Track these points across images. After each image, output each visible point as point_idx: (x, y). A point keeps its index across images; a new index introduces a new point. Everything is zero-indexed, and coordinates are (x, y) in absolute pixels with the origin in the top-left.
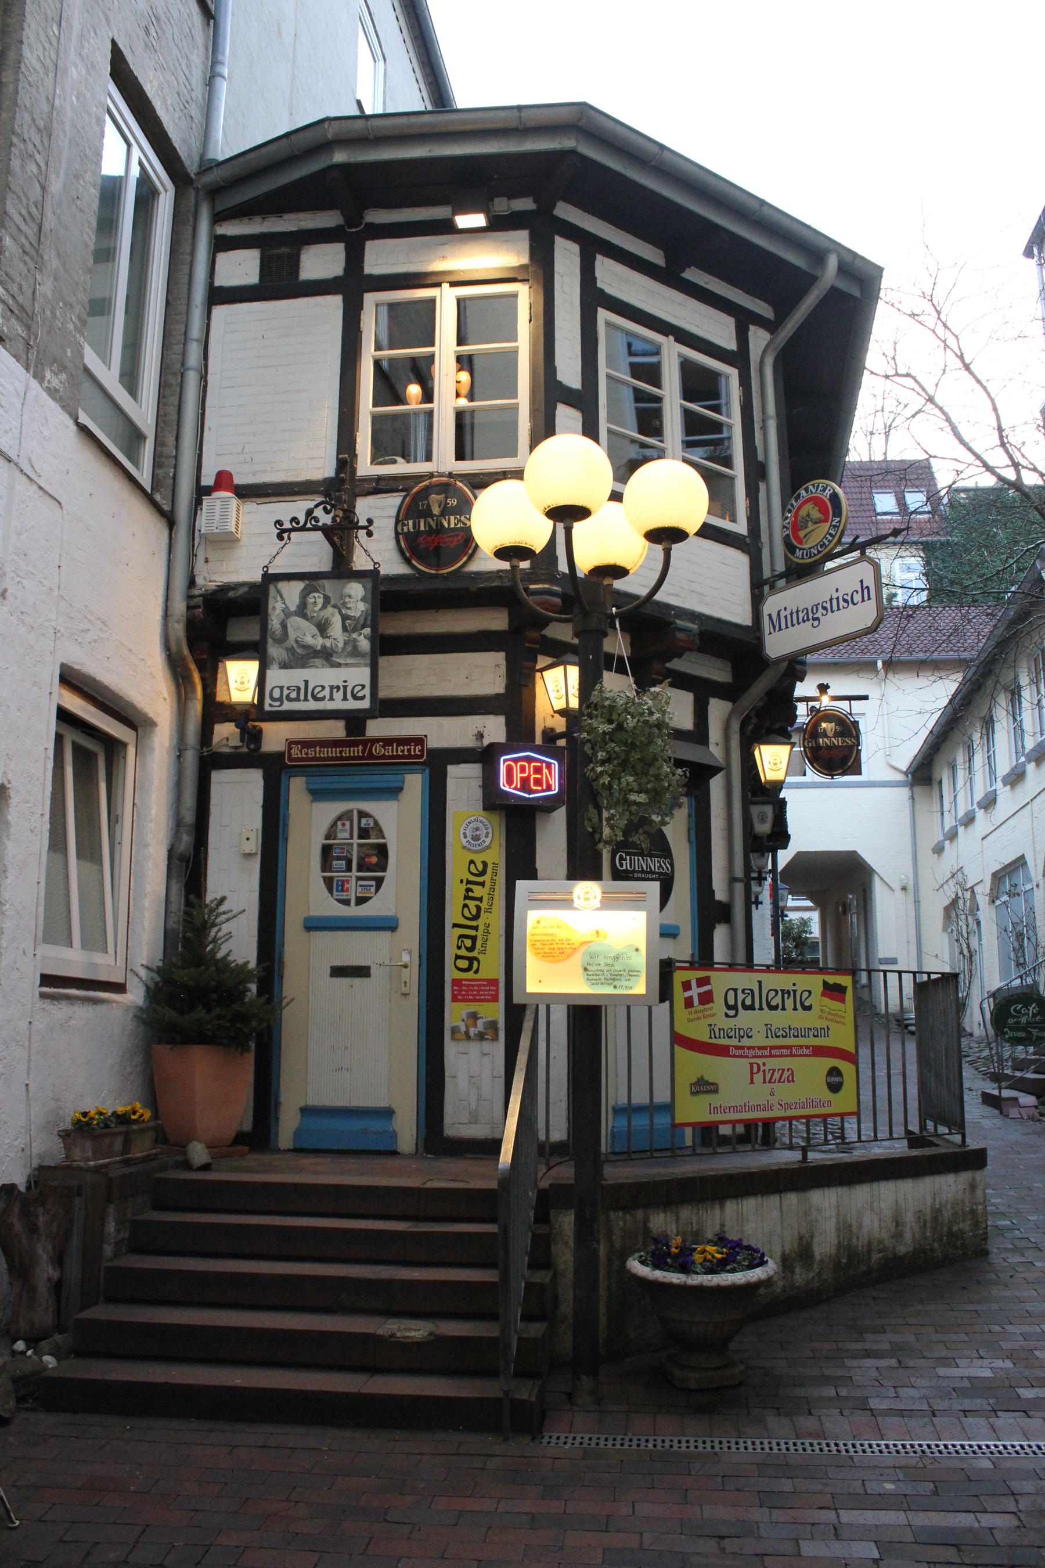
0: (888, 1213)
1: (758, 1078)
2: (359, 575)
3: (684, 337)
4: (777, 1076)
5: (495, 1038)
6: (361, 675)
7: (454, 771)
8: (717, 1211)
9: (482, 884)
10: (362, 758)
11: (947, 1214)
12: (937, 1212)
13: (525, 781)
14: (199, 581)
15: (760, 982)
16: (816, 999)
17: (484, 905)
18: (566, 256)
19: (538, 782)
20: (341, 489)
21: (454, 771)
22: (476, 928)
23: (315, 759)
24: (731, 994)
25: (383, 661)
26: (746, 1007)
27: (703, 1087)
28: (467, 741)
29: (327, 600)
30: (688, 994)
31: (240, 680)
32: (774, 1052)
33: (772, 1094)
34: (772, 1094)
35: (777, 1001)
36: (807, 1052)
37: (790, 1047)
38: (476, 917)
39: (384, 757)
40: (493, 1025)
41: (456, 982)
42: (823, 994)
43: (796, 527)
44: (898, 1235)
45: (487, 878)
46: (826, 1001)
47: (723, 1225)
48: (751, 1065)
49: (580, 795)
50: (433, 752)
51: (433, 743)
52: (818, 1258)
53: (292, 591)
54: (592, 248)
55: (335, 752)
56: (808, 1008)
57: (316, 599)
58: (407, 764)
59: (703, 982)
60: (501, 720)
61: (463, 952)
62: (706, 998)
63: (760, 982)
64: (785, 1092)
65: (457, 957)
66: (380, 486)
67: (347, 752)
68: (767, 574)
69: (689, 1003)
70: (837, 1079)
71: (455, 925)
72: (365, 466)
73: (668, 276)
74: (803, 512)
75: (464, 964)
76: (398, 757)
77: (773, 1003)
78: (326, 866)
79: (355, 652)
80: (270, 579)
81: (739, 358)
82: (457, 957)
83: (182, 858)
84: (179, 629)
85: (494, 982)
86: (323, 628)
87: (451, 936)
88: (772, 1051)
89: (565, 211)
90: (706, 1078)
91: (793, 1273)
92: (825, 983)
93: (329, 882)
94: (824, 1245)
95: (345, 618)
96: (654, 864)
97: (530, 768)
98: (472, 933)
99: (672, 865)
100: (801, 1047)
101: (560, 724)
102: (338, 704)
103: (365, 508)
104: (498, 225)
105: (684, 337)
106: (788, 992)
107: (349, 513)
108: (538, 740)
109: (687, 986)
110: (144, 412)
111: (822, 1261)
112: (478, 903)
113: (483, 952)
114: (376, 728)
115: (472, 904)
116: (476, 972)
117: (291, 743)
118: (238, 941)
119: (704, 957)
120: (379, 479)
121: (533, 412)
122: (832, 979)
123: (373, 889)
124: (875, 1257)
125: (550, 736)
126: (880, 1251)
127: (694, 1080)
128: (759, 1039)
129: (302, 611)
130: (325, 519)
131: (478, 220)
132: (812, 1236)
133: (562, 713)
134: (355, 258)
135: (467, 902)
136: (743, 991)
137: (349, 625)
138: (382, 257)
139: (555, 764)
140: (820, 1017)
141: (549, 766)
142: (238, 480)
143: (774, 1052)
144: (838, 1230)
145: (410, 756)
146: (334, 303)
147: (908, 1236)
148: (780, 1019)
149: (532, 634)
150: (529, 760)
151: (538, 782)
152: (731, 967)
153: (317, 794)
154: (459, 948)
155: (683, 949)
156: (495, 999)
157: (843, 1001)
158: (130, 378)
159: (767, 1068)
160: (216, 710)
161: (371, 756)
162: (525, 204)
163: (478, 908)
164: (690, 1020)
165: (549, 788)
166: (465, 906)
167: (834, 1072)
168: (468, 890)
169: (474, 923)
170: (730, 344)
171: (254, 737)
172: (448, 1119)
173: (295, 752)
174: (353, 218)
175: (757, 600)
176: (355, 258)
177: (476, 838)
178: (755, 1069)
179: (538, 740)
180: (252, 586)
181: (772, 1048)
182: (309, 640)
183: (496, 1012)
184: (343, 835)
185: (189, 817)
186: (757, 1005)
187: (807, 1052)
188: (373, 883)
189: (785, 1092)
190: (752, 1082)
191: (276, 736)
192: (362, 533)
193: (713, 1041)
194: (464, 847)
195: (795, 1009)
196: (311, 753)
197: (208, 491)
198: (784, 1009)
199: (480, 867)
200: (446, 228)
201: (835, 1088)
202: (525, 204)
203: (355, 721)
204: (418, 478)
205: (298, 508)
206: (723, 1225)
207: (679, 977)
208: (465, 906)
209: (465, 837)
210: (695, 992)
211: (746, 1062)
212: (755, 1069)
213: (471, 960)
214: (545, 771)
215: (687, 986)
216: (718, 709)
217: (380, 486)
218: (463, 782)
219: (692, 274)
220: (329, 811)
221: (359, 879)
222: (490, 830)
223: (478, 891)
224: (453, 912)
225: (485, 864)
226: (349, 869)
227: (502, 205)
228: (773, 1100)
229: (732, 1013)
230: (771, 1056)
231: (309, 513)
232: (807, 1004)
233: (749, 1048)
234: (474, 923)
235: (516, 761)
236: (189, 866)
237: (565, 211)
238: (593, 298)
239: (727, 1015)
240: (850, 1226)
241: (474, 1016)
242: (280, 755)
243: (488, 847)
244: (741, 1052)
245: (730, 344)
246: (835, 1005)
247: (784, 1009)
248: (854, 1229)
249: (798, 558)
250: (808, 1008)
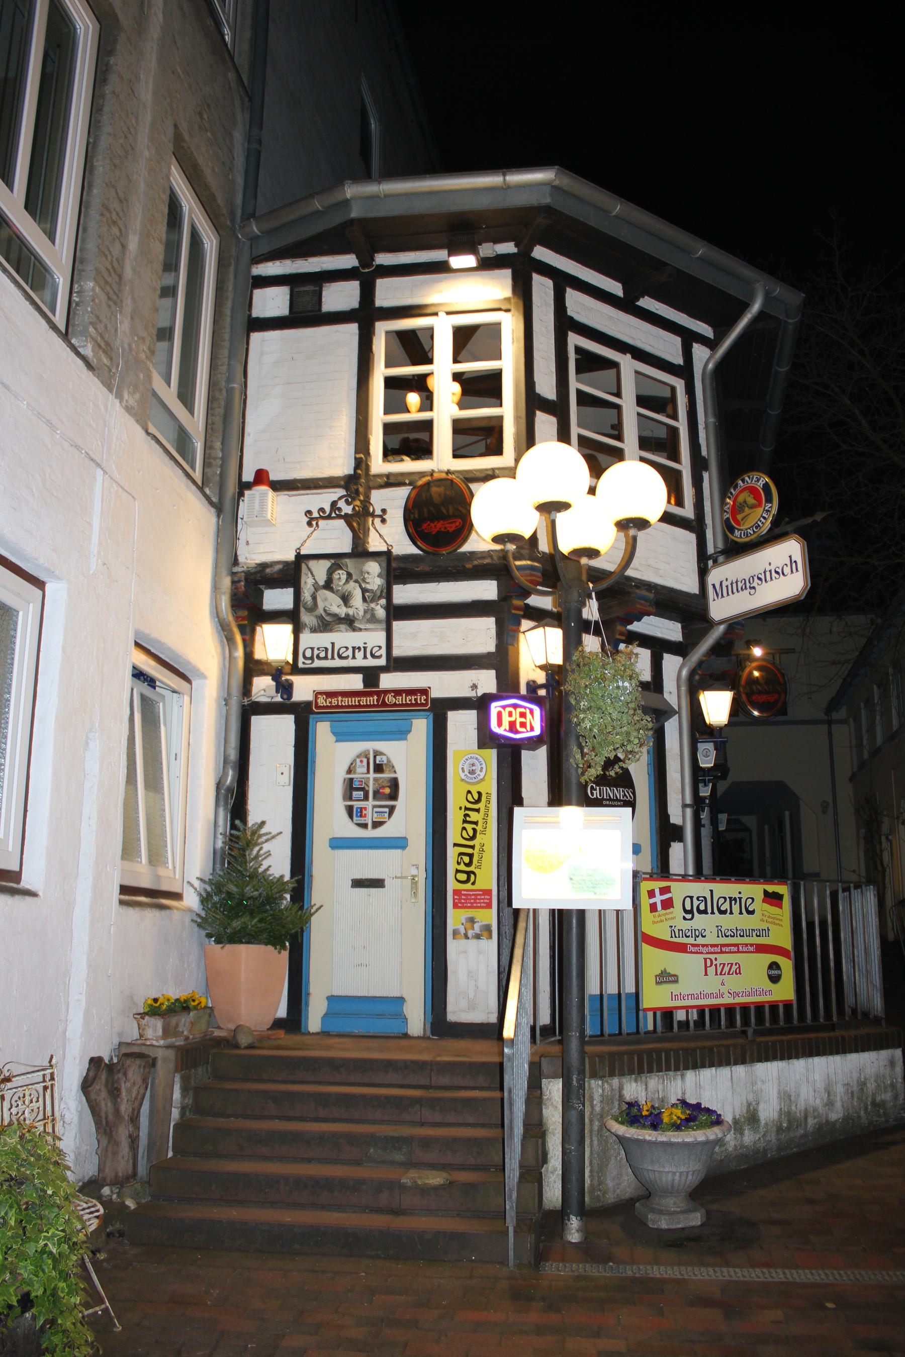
0: (820, 1086)
1: (711, 970)
2: (376, 555)
3: (639, 354)
4: (726, 969)
5: (490, 937)
6: (377, 638)
7: (454, 717)
8: (679, 1081)
9: (478, 810)
10: (377, 706)
11: (871, 1086)
12: (863, 1084)
13: (512, 725)
14: (241, 559)
15: (712, 891)
16: (758, 905)
17: (479, 828)
18: (543, 288)
19: (523, 725)
20: (357, 483)
21: (454, 717)
22: (473, 847)
23: (337, 706)
24: (688, 900)
25: (396, 625)
26: (700, 912)
27: (666, 978)
28: (465, 692)
29: (349, 575)
30: (652, 901)
31: (275, 642)
32: (724, 949)
33: (723, 984)
34: (723, 984)
35: (726, 906)
36: (752, 949)
37: (737, 945)
38: (473, 838)
39: (395, 705)
40: (488, 928)
41: (456, 892)
42: (764, 901)
43: (735, 511)
44: (830, 1104)
45: (481, 806)
46: (766, 906)
47: (684, 1093)
48: (705, 960)
49: (556, 736)
50: (435, 701)
51: (435, 694)
52: (763, 1122)
53: (320, 569)
54: (563, 282)
55: (354, 701)
57: (340, 576)
58: (414, 708)
59: (664, 891)
60: (493, 673)
61: (462, 867)
63: (712, 891)
64: (734, 983)
65: (458, 871)
66: (391, 481)
67: (364, 701)
68: (710, 550)
69: (653, 908)
70: (776, 972)
71: (455, 845)
72: (378, 465)
73: (626, 304)
74: (741, 499)
75: (463, 877)
77: (723, 908)
78: (348, 796)
79: (373, 619)
80: (301, 558)
81: (685, 371)
82: (458, 871)
83: (229, 790)
84: (225, 602)
85: (488, 892)
86: (346, 599)
87: (452, 853)
88: (722, 949)
89: (541, 253)
91: (742, 1134)
92: (765, 892)
93: (350, 810)
94: (769, 1112)
95: (364, 591)
96: (619, 793)
97: (516, 713)
98: (469, 851)
99: (634, 793)
100: (747, 945)
101: (541, 677)
102: (359, 662)
103: (379, 499)
104: (487, 264)
105: (639, 354)
106: (735, 899)
107: (366, 502)
108: (523, 691)
109: (651, 894)
110: (196, 424)
111: (766, 1124)
112: (474, 826)
113: (479, 867)
114: (388, 681)
115: (469, 827)
116: (473, 883)
117: (317, 694)
118: (276, 860)
119: (662, 869)
120: (388, 476)
121: (517, 418)
122: (771, 888)
123: (387, 815)
124: (811, 1122)
125: (533, 687)
126: (815, 1118)
128: (711, 939)
129: (328, 585)
130: (347, 509)
131: (469, 261)
132: (758, 1104)
133: (542, 667)
134: (367, 293)
135: (465, 825)
136: (698, 898)
137: (368, 597)
138: (388, 292)
139: (537, 711)
140: (762, 920)
141: (532, 712)
142: (273, 477)
143: (724, 949)
144: (780, 1098)
145: (416, 704)
146: (352, 330)
147: (838, 1104)
148: (728, 922)
149: (517, 602)
150: (515, 706)
151: (523, 725)
152: (684, 878)
153: (341, 736)
155: (647, 864)
156: (489, 906)
157: (780, 907)
158: (186, 396)
160: (253, 667)
161: (384, 704)
162: (508, 248)
163: (474, 830)
164: (654, 922)
165: (532, 729)
166: (464, 828)
167: (774, 966)
168: (466, 815)
170: (679, 360)
171: (286, 689)
172: (450, 1007)
173: (321, 701)
174: (366, 259)
175: (703, 573)
176: (367, 293)
177: (472, 772)
178: (708, 961)
179: (523, 691)
180: (286, 564)
181: (723, 945)
182: (335, 609)
183: (490, 916)
184: (361, 769)
185: (233, 755)
186: (709, 910)
187: (752, 949)
188: (387, 810)
189: (734, 983)
190: (706, 974)
191: (304, 688)
192: (377, 521)
193: (674, 940)
194: (463, 780)
195: (741, 913)
196: (334, 702)
197: (248, 486)
198: (731, 913)
199: (476, 796)
200: (442, 268)
201: (775, 979)
202: (508, 248)
203: (371, 675)
204: (422, 474)
205: (323, 499)
206: (684, 1093)
207: (646, 886)
208: (464, 828)
209: (463, 771)
210: (658, 899)
211: (701, 957)
212: (708, 961)
213: (469, 873)
214: (529, 715)
215: (651, 894)
216: (671, 664)
217: (391, 481)
218: (462, 726)
219: (646, 303)
220: (351, 750)
221: (374, 807)
222: (484, 766)
223: (474, 816)
224: (453, 834)
225: (480, 793)
226: (366, 798)
227: (488, 250)
228: (724, 990)
229: (689, 916)
230: (722, 952)
231: (334, 504)
232: (750, 909)
233: (703, 946)
235: (504, 707)
236: (235, 799)
237: (541, 253)
238: (565, 324)
239: (685, 918)
240: (790, 1096)
241: (472, 920)
242: (308, 704)
243: (482, 780)
244: (697, 949)
245: (679, 360)
246: (774, 910)
248: (793, 1098)
249: (738, 536)
250: (751, 913)
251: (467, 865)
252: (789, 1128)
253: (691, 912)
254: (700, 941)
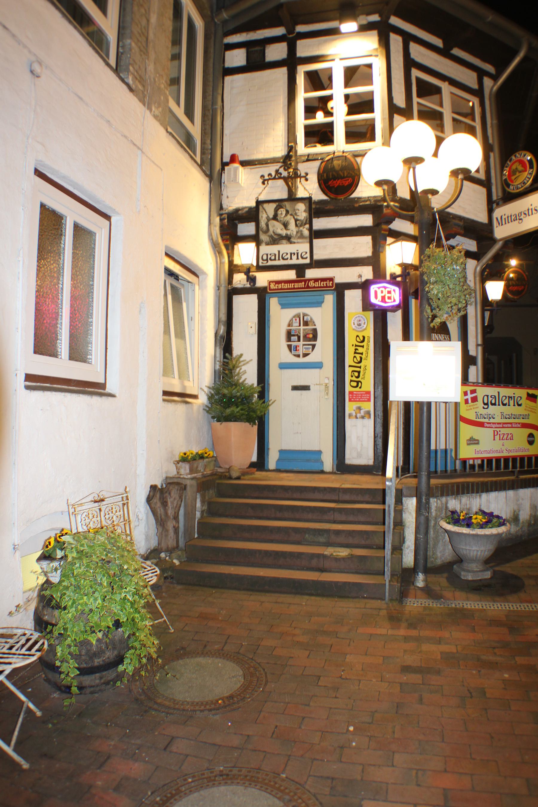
1: (497, 437)
4: (505, 437)
5: (370, 417)
8: (478, 499)
10: (304, 288)
13: (383, 298)
15: (499, 392)
16: (524, 401)
17: (363, 357)
19: (389, 298)
22: (360, 367)
23: (281, 289)
24: (486, 397)
26: (492, 404)
27: (473, 441)
30: (466, 397)
32: (504, 426)
33: (503, 445)
34: (503, 445)
35: (506, 401)
36: (519, 426)
38: (360, 362)
39: (314, 287)
40: (368, 413)
42: (527, 399)
46: (528, 402)
47: (480, 506)
48: (494, 431)
56: (520, 405)
58: (325, 289)
61: (354, 378)
62: (475, 399)
63: (499, 392)
65: (351, 381)
67: (297, 285)
70: (531, 439)
71: (350, 366)
76: (321, 287)
77: (504, 402)
82: (351, 381)
88: (503, 425)
90: (474, 437)
92: (528, 394)
98: (358, 369)
100: (517, 423)
106: (511, 397)
112: (361, 355)
113: (363, 378)
115: (358, 356)
116: (360, 388)
118: (249, 375)
122: (531, 392)
123: (311, 350)
127: (469, 438)
128: (498, 420)
132: (519, 511)
135: (356, 355)
136: (491, 397)
139: (397, 289)
140: (525, 410)
141: (394, 290)
143: (504, 426)
145: (327, 287)
151: (389, 298)
156: (369, 400)
159: (501, 433)
161: (308, 287)
163: (361, 358)
165: (394, 301)
166: (355, 357)
167: (531, 435)
168: (356, 349)
169: (359, 365)
177: (359, 325)
178: (496, 434)
183: (369, 406)
186: (497, 403)
187: (519, 426)
188: (311, 347)
190: (494, 440)
194: (354, 329)
195: (514, 405)
198: (509, 405)
206: (480, 506)
208: (355, 357)
209: (354, 324)
211: (491, 430)
212: (496, 434)
213: (358, 382)
214: (392, 292)
218: (353, 298)
221: (304, 345)
222: (366, 321)
223: (360, 350)
224: (349, 360)
228: (504, 448)
229: (486, 407)
230: (503, 427)
232: (520, 403)
233: (493, 423)
234: (359, 365)
239: (484, 408)
241: (359, 408)
243: (365, 329)
244: (489, 425)
247: (509, 405)
252: (534, 524)
253: (487, 404)
254: (492, 421)
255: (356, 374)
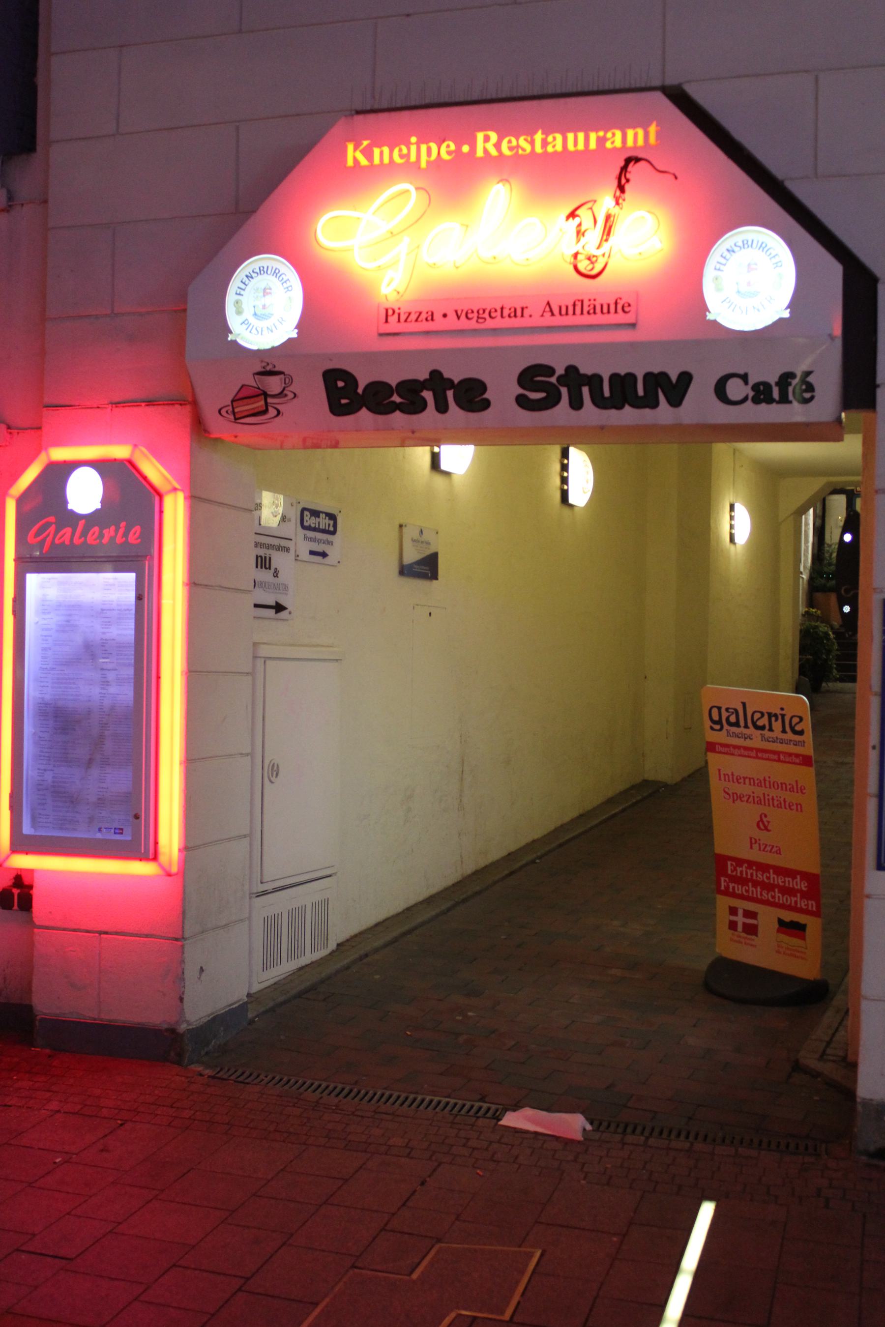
9: (784, 731)
22: (746, 727)
45: (790, 735)
61: (725, 715)
98: (742, 723)
112: (767, 727)
115: (764, 721)
135: (766, 716)
154: (727, 710)
163: (762, 728)
169: (750, 724)
199: (798, 728)
223: (777, 725)
225: (801, 733)
234: (750, 724)
251: (727, 719)
255: (733, 719)
